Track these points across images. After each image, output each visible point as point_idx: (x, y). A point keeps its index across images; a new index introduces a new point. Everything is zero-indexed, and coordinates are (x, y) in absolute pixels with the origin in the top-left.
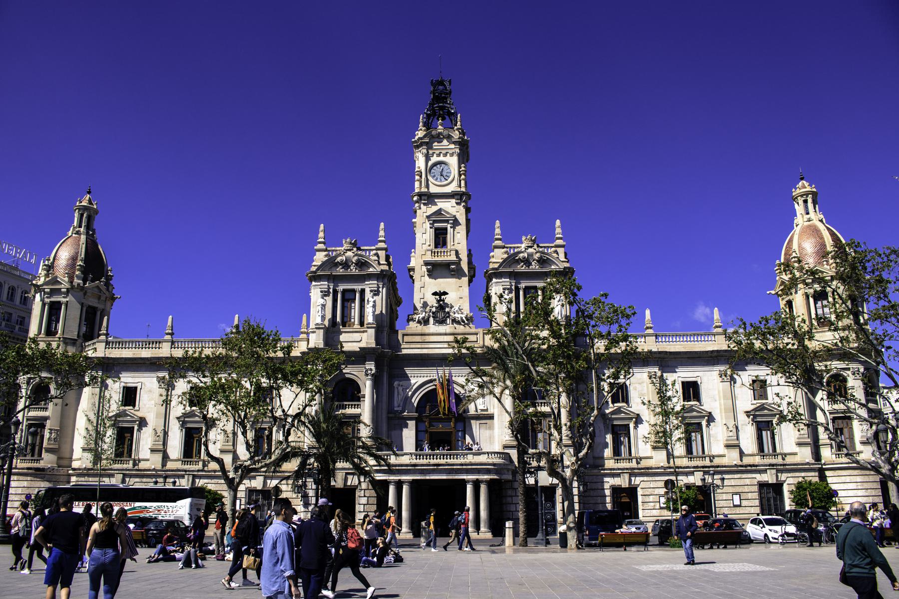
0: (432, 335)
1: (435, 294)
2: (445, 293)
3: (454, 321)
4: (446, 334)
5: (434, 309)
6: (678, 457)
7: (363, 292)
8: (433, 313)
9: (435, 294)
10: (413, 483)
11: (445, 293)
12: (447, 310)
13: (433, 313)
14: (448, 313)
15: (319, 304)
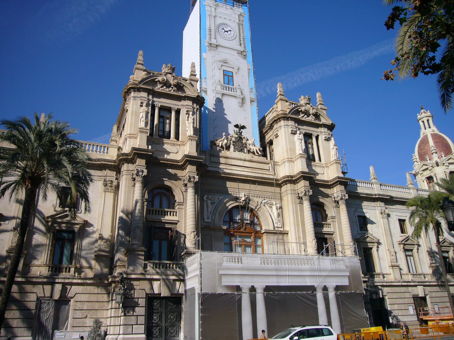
0: (234, 159)
1: (236, 126)
2: (243, 127)
3: (249, 151)
4: (245, 160)
5: (234, 139)
6: (404, 274)
7: (178, 112)
8: (234, 142)
9: (236, 126)
10: (267, 289)
11: (243, 127)
12: (244, 141)
13: (234, 142)
14: (246, 144)
15: (136, 113)
